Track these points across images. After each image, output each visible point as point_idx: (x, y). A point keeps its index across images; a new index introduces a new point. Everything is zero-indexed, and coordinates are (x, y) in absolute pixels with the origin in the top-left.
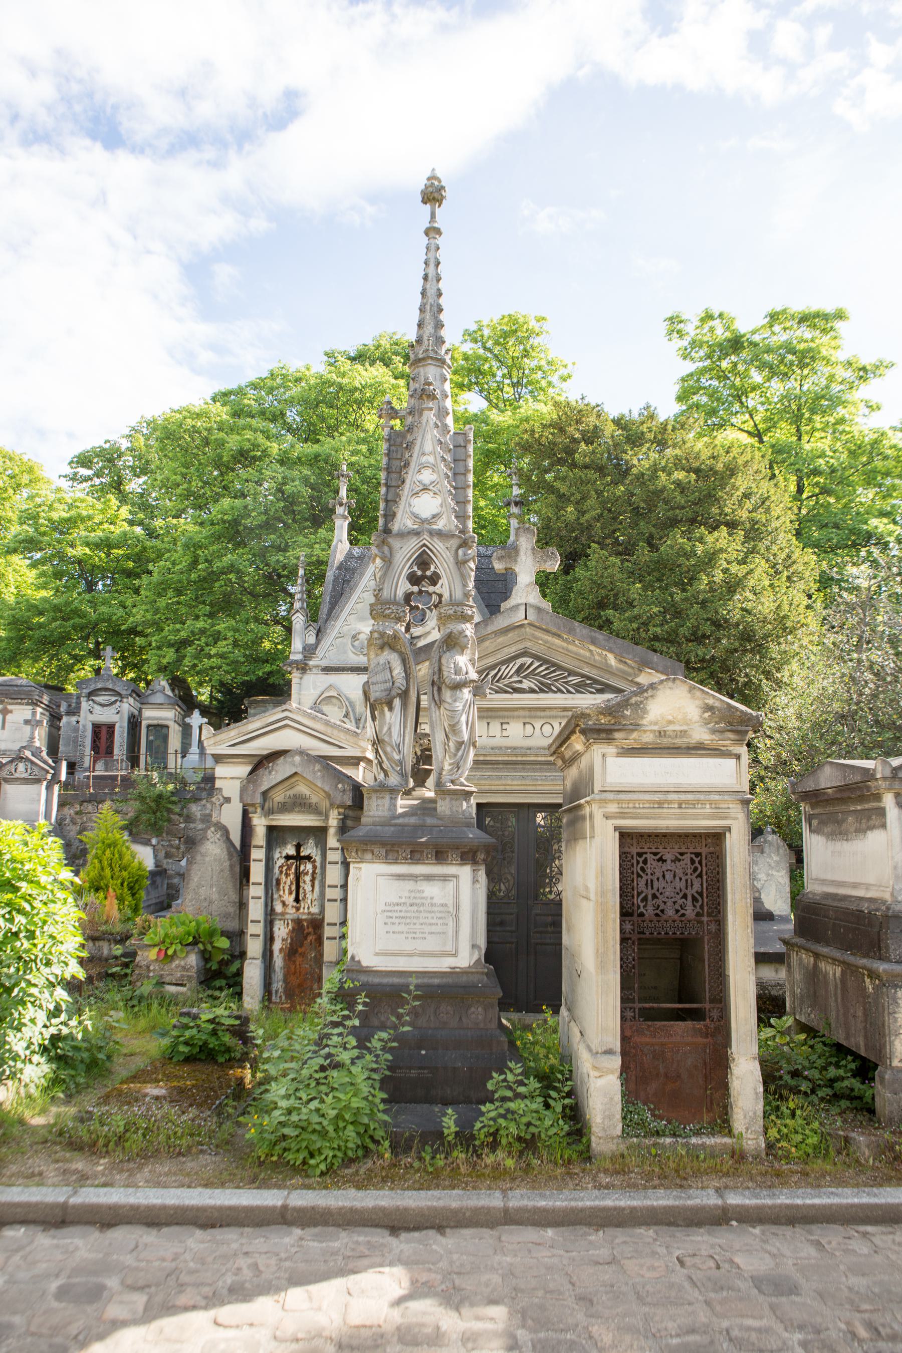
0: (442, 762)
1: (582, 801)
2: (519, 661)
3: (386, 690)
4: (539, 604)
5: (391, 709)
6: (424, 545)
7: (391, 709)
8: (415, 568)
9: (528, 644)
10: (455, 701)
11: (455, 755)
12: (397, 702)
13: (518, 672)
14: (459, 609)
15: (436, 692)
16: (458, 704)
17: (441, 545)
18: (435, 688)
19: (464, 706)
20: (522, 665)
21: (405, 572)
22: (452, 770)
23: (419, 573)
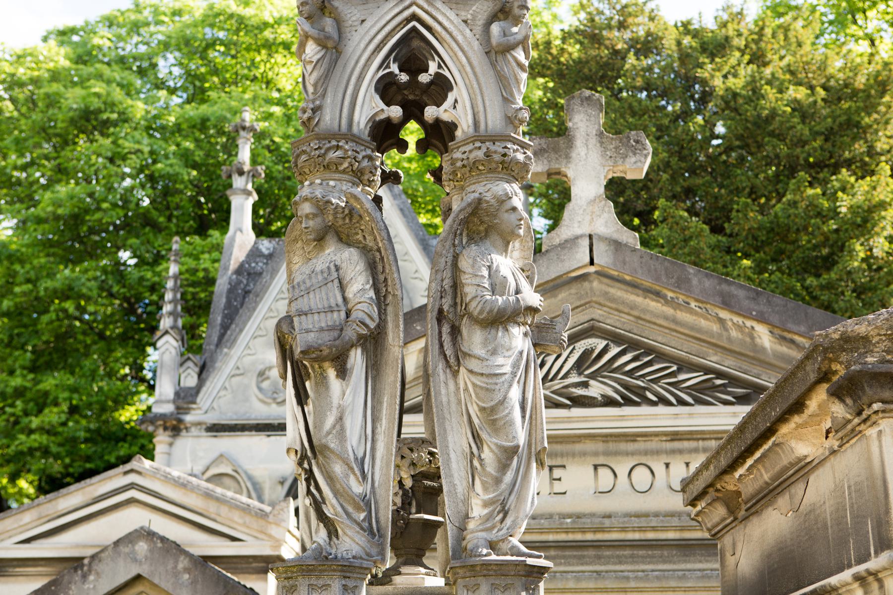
0: (466, 501)
1: (846, 575)
2: (581, 346)
3: (331, 329)
4: (616, 236)
5: (343, 373)
6: (414, 17)
7: (343, 373)
8: (394, 68)
9: (597, 313)
10: (494, 352)
11: (498, 481)
12: (357, 359)
13: (579, 366)
14: (498, 147)
15: (446, 338)
16: (500, 360)
17: (451, 15)
18: (446, 329)
19: (516, 366)
20: (586, 354)
21: (372, 74)
22: (489, 517)
23: (404, 77)
